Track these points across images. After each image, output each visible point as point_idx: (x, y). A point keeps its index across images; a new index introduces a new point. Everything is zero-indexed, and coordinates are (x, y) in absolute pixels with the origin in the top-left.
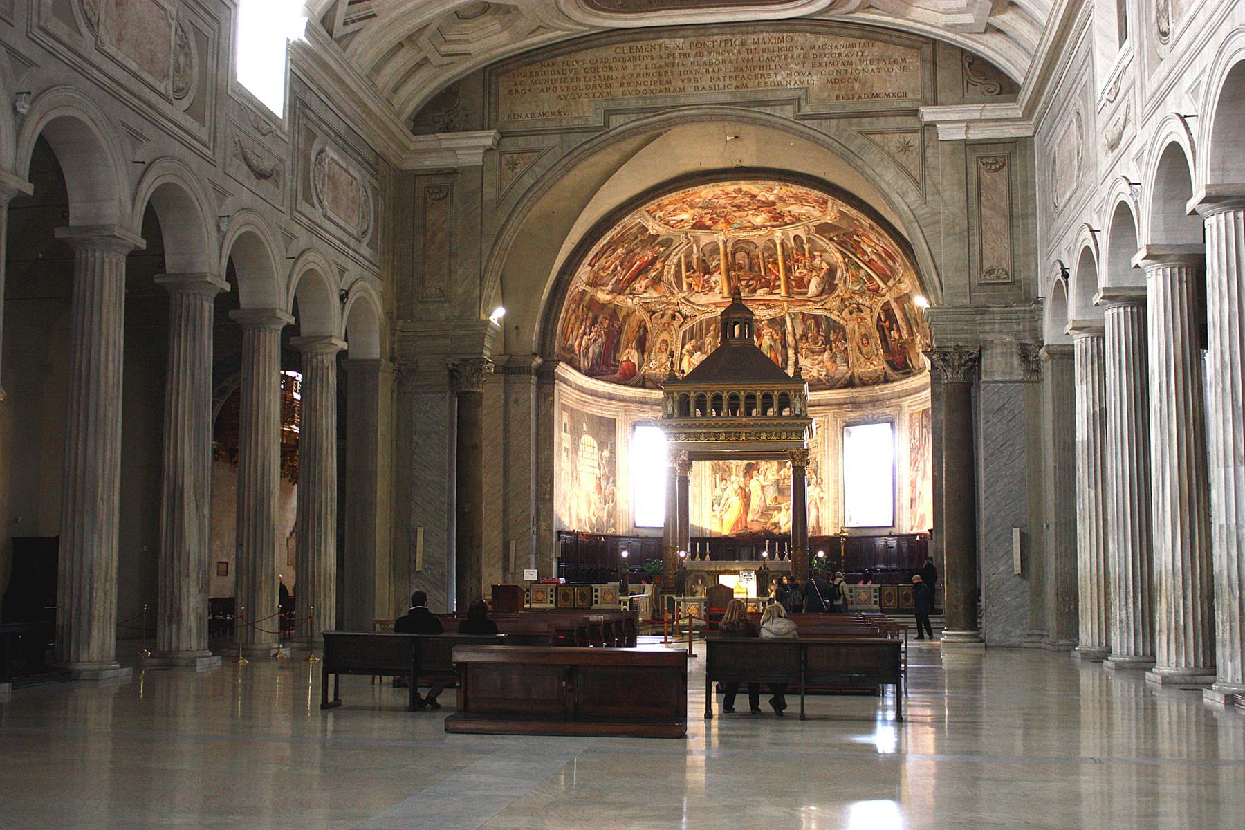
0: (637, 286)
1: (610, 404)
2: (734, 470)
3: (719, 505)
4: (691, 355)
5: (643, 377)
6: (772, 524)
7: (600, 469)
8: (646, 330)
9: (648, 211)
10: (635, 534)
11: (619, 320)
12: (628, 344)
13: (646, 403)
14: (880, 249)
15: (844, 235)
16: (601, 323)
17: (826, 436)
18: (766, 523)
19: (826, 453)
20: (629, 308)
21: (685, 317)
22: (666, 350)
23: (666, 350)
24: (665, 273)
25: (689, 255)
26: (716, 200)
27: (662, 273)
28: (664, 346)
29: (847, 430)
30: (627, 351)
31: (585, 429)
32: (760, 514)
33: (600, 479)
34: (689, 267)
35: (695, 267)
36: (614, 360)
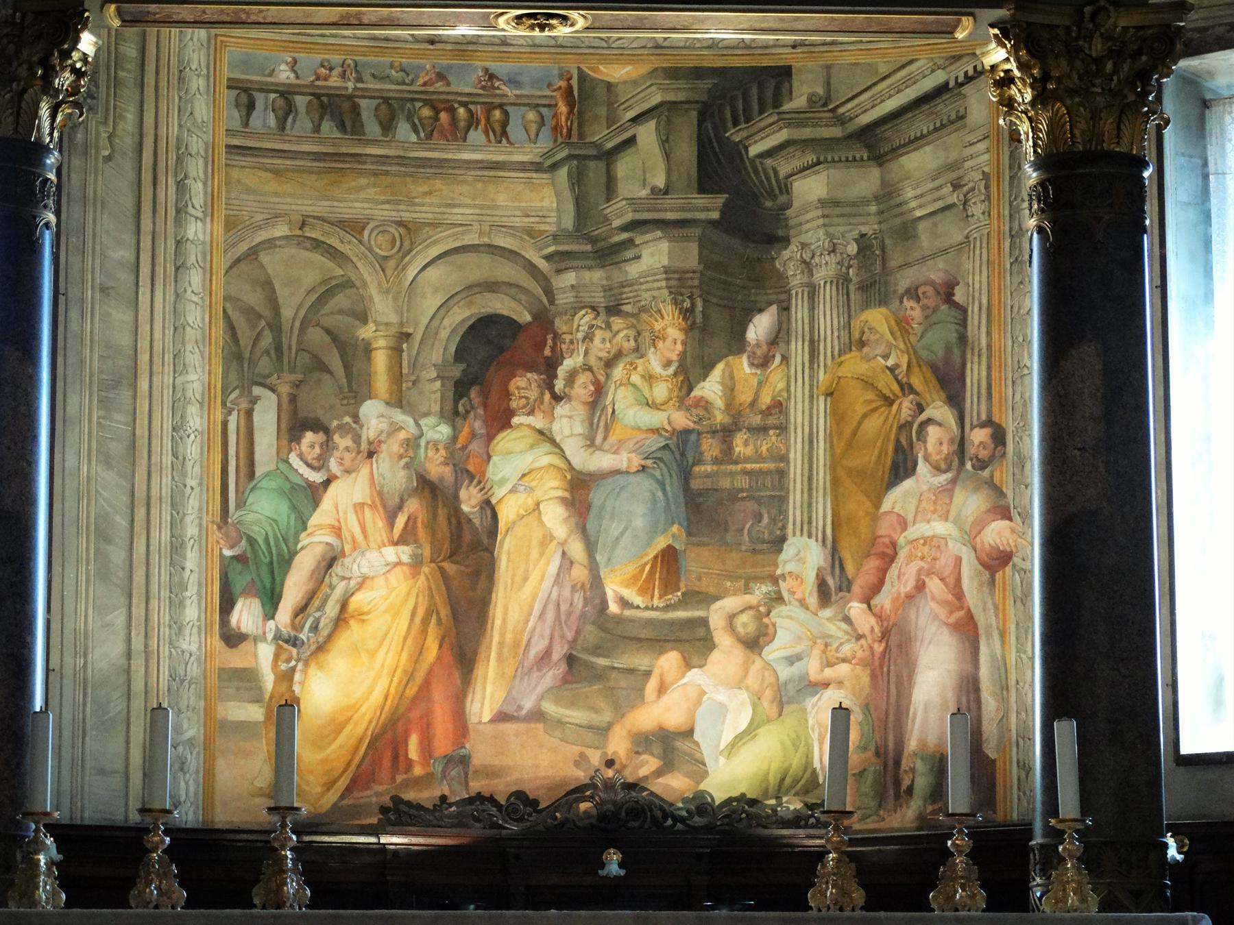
2: (381, 360)
3: (272, 600)
6: (643, 741)
18: (603, 731)
32: (551, 676)
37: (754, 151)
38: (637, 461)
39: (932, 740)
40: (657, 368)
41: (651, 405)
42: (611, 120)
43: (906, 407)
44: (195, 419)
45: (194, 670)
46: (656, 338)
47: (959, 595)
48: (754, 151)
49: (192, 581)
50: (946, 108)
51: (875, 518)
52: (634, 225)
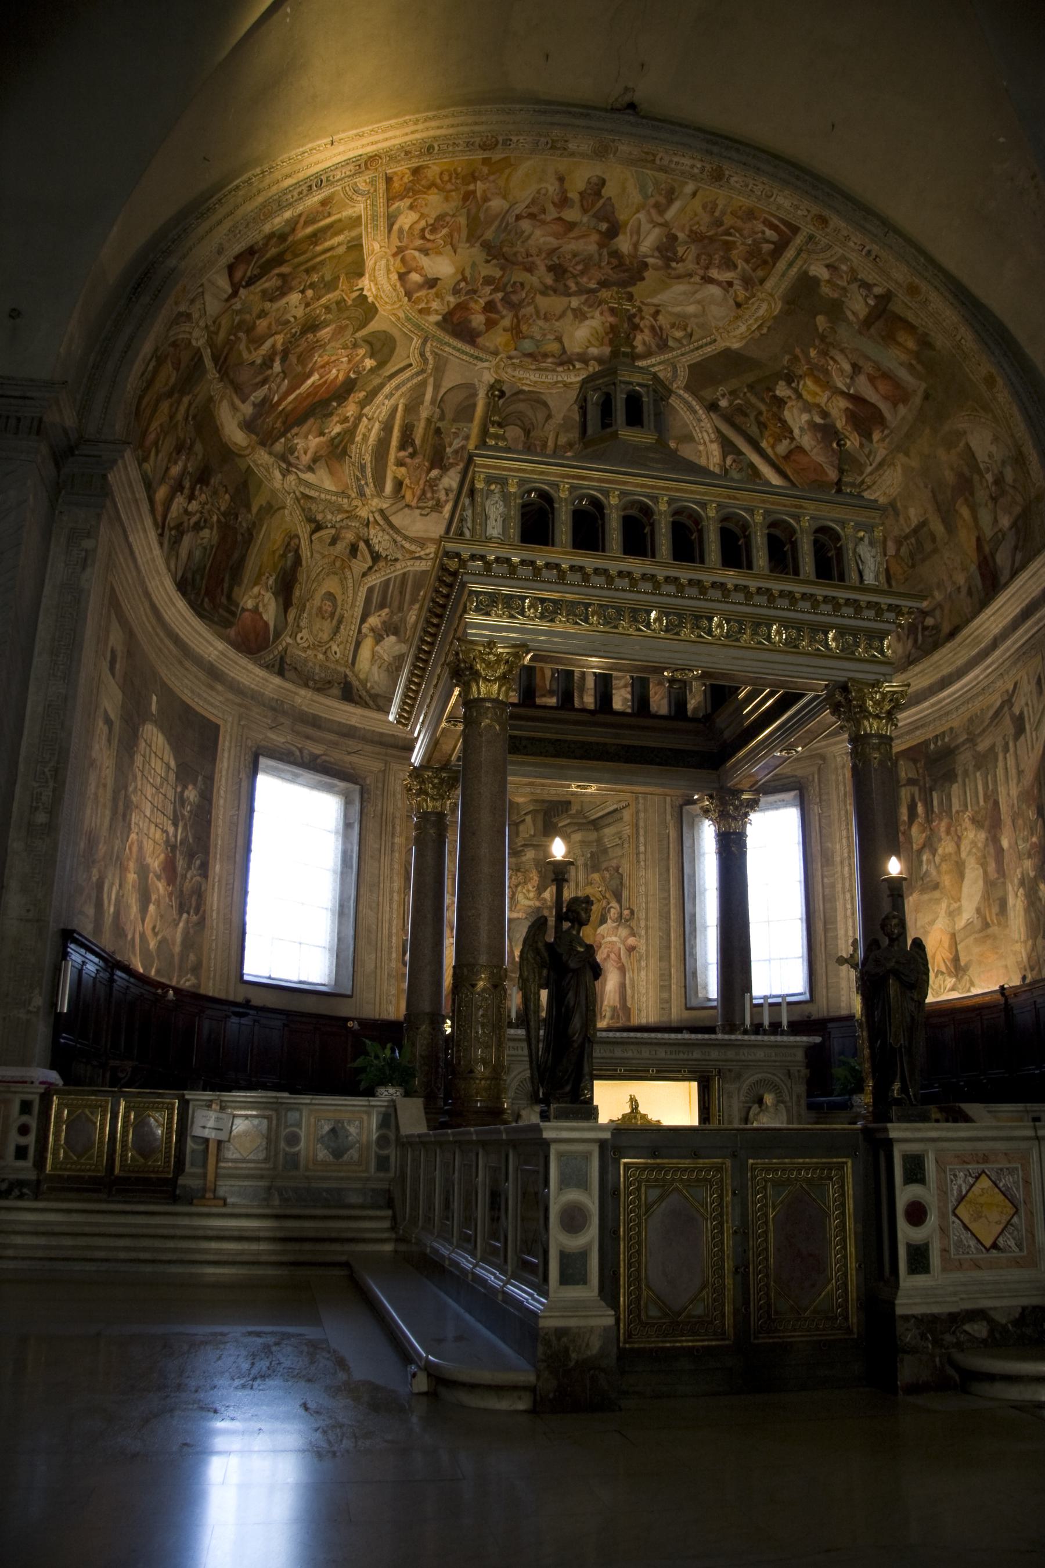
0: (300, 443)
1: (212, 688)
4: (379, 639)
5: (282, 659)
7: (175, 825)
8: (298, 561)
9: (389, 180)
10: (240, 999)
11: (249, 511)
12: (260, 575)
13: (284, 713)
14: (838, 408)
15: (751, 387)
16: (215, 493)
17: (641, 824)
19: (642, 857)
20: (273, 492)
21: (376, 557)
22: (332, 615)
23: (332, 615)
24: (358, 438)
25: (411, 408)
26: (526, 225)
27: (351, 432)
28: (328, 606)
29: (688, 812)
30: (256, 590)
31: (154, 708)
33: (174, 848)
34: (406, 441)
35: (418, 442)
36: (229, 597)
37: (560, 825)
38: (524, 916)
39: (611, 1003)
40: (530, 888)
41: (528, 899)
42: (518, 814)
43: (604, 903)
44: (396, 897)
45: (394, 973)
46: (531, 879)
47: (620, 958)
48: (560, 825)
49: (394, 945)
50: (617, 816)
51: (595, 935)
52: (522, 846)
